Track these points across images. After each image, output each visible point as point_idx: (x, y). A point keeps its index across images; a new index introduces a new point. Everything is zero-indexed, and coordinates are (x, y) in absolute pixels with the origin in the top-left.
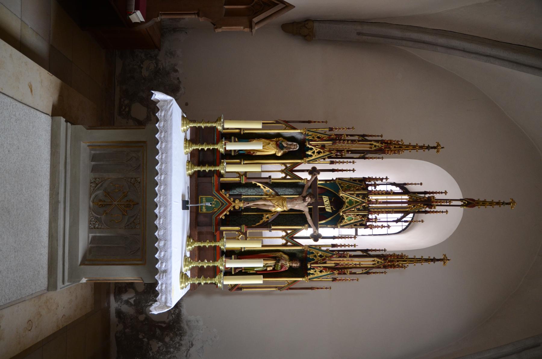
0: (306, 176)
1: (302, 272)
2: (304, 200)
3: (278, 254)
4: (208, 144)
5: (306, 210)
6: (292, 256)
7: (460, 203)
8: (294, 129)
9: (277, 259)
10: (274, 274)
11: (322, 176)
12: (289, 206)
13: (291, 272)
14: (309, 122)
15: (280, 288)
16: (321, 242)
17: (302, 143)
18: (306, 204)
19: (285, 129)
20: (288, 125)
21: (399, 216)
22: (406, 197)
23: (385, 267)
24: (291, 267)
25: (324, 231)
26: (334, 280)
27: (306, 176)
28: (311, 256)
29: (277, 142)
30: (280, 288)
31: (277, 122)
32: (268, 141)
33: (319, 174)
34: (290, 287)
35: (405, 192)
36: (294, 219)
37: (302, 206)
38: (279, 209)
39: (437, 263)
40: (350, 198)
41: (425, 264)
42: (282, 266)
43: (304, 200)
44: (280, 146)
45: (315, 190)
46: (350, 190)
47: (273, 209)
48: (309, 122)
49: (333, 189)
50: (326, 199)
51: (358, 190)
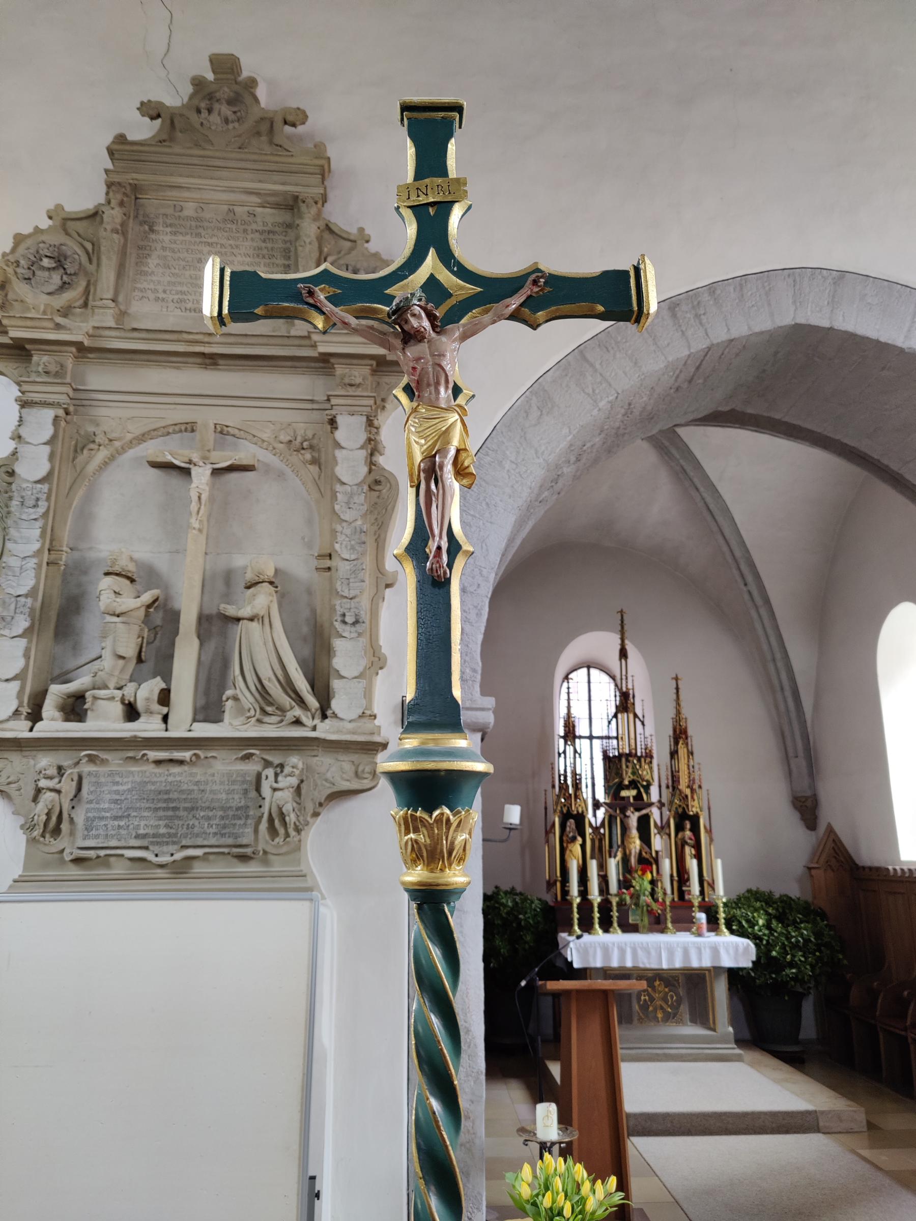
0: (601, 813)
1: (695, 820)
2: (628, 817)
3: (679, 843)
4: (592, 912)
5: (637, 814)
6: (679, 828)
7: (623, 661)
8: (553, 825)
9: (684, 843)
10: (697, 846)
11: (601, 796)
12: (634, 833)
13: (695, 829)
14: (546, 808)
15: (711, 840)
16: (664, 800)
17: (566, 816)
18: (632, 815)
19: (555, 834)
20: (549, 831)
21: (638, 723)
22: (619, 716)
23: (687, 738)
24: (691, 830)
25: (654, 797)
26: (700, 787)
27: (601, 813)
28: (680, 810)
29: (568, 842)
30: (711, 840)
31: (547, 841)
32: (568, 852)
33: (598, 801)
34: (709, 831)
35: (615, 716)
36: (644, 824)
37: (633, 819)
38: (638, 842)
39: (680, 686)
40: (629, 774)
41: (681, 697)
42: (691, 839)
43: (628, 817)
44: (574, 839)
45: (617, 805)
46: (622, 775)
47: (638, 847)
48: (546, 808)
49: (614, 786)
50: (624, 793)
51: (621, 766)
